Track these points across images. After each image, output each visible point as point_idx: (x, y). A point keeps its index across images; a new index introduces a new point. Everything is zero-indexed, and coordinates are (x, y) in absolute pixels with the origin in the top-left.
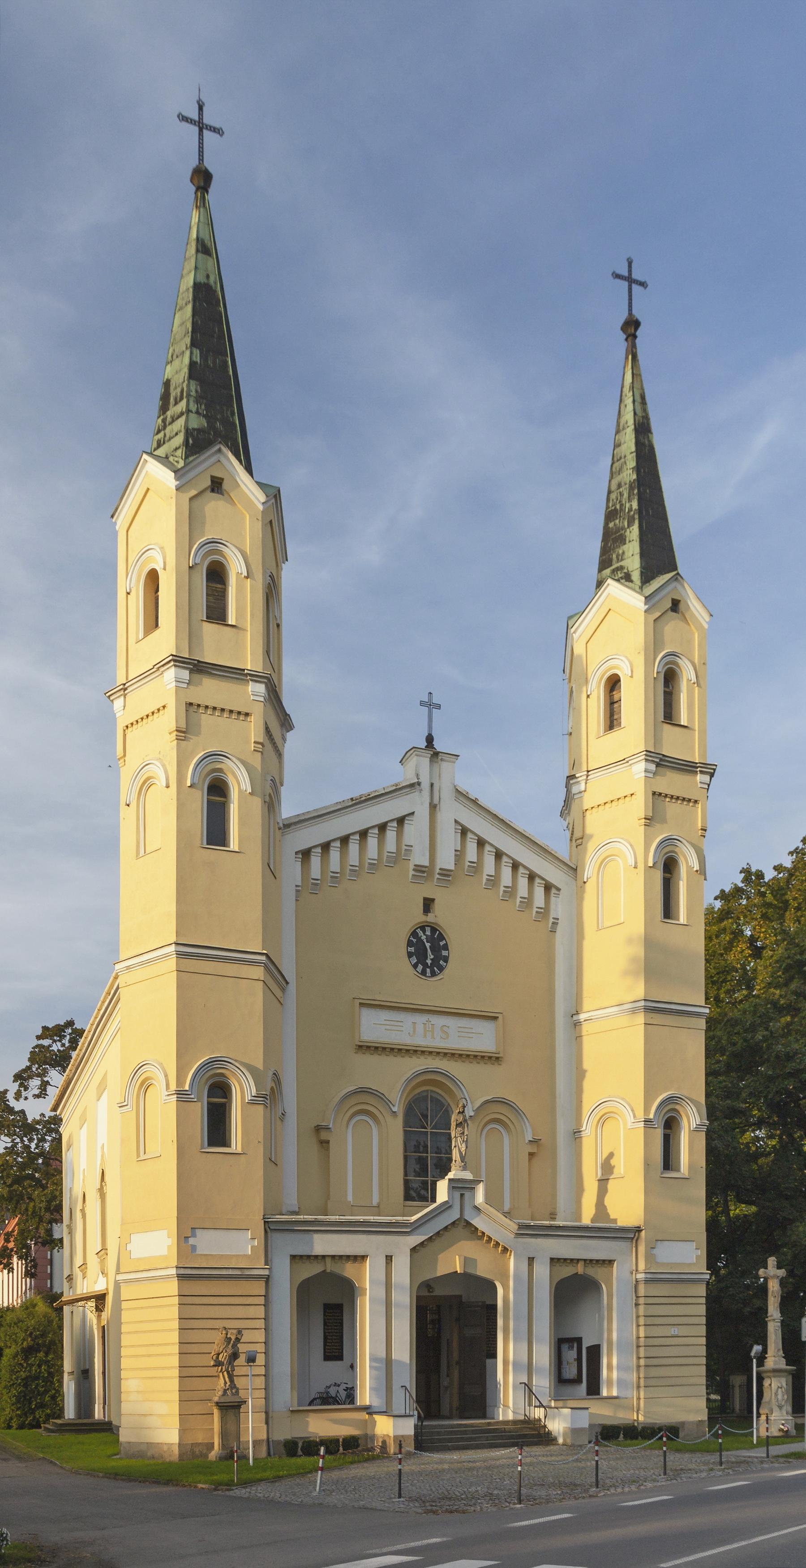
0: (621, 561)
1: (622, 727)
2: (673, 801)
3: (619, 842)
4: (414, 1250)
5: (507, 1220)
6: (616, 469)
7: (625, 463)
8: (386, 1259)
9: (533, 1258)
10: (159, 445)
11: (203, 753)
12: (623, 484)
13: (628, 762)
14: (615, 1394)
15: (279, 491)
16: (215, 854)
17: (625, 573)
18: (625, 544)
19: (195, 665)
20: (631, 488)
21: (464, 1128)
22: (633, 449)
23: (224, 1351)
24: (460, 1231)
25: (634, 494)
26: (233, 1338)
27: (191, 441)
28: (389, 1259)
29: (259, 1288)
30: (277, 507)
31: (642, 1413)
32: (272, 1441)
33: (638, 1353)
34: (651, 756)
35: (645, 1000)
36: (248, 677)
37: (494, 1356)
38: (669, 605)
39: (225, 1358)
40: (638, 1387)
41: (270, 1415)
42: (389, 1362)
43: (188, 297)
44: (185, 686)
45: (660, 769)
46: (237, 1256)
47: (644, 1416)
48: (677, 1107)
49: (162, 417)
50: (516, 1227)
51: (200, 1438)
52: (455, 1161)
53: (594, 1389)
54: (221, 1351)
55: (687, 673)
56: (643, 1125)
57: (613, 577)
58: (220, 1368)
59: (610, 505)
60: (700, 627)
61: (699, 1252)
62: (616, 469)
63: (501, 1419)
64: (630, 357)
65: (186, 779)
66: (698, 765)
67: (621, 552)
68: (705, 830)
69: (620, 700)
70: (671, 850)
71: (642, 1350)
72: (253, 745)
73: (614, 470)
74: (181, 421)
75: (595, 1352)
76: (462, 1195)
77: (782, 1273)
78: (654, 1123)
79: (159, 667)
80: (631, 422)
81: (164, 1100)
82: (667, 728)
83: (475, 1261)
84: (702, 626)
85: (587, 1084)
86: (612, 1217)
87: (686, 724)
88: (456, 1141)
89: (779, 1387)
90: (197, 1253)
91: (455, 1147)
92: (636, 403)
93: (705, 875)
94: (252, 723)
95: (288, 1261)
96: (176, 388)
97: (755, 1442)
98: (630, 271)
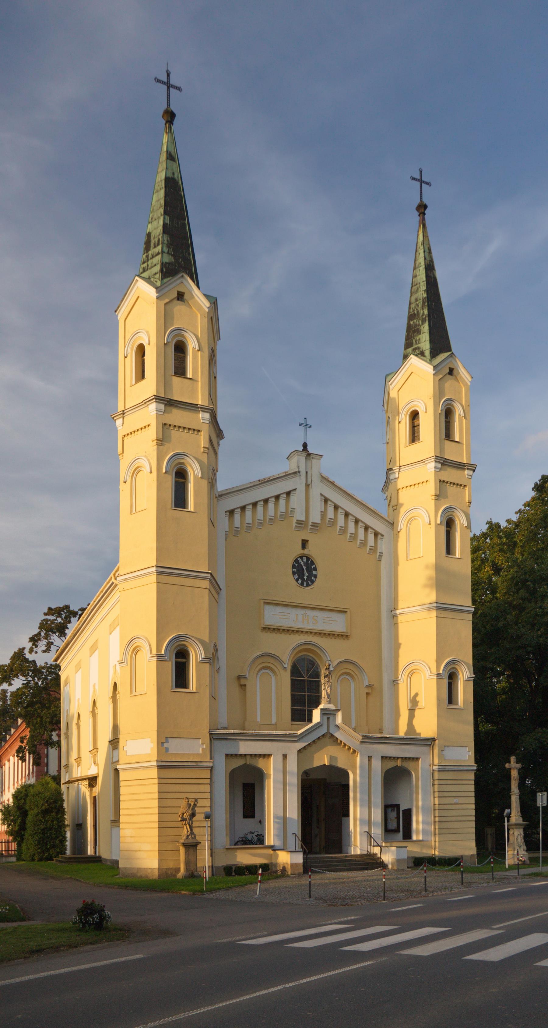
0: (418, 344)
1: (420, 441)
2: (452, 485)
3: (419, 509)
4: (299, 751)
5: (356, 734)
6: (414, 290)
7: (420, 287)
8: (283, 757)
9: (371, 756)
10: (144, 270)
11: (172, 453)
12: (418, 299)
13: (424, 462)
14: (421, 838)
15: (216, 300)
16: (179, 513)
17: (421, 351)
18: (420, 334)
19: (168, 402)
20: (423, 302)
21: (329, 678)
22: (424, 279)
23: (187, 812)
24: (327, 740)
25: (425, 306)
26: (192, 804)
27: (164, 270)
28: (285, 756)
29: (207, 774)
30: (215, 309)
31: (438, 850)
32: (215, 867)
33: (434, 814)
34: (438, 459)
35: (436, 603)
36: (200, 409)
37: (347, 815)
38: (448, 371)
39: (188, 816)
40: (435, 834)
41: (214, 850)
42: (285, 818)
43: (162, 185)
44: (162, 413)
45: (444, 467)
47: (439, 852)
48: (456, 666)
49: (146, 254)
50: (361, 738)
51: (171, 865)
52: (324, 698)
53: (407, 835)
54: (185, 812)
55: (458, 411)
56: (436, 677)
57: (414, 353)
58: (184, 822)
59: (411, 311)
60: (465, 384)
61: (470, 753)
62: (414, 290)
63: (352, 853)
64: (422, 226)
65: (163, 469)
66: (466, 465)
67: (418, 338)
68: (471, 503)
69: (419, 425)
70: (449, 514)
71: (437, 812)
72: (202, 449)
73: (413, 290)
74: (158, 258)
75: (408, 814)
76: (328, 718)
77: (519, 766)
79: (146, 402)
80: (423, 263)
81: (150, 660)
82: (447, 442)
83: (336, 758)
84: (467, 384)
85: (402, 652)
87: (458, 441)
88: (324, 686)
89: (518, 835)
90: (169, 752)
91: (324, 689)
92: (426, 253)
93: (471, 529)
94: (202, 436)
95: (224, 757)
96: (154, 238)
97: (507, 867)
98: (421, 176)
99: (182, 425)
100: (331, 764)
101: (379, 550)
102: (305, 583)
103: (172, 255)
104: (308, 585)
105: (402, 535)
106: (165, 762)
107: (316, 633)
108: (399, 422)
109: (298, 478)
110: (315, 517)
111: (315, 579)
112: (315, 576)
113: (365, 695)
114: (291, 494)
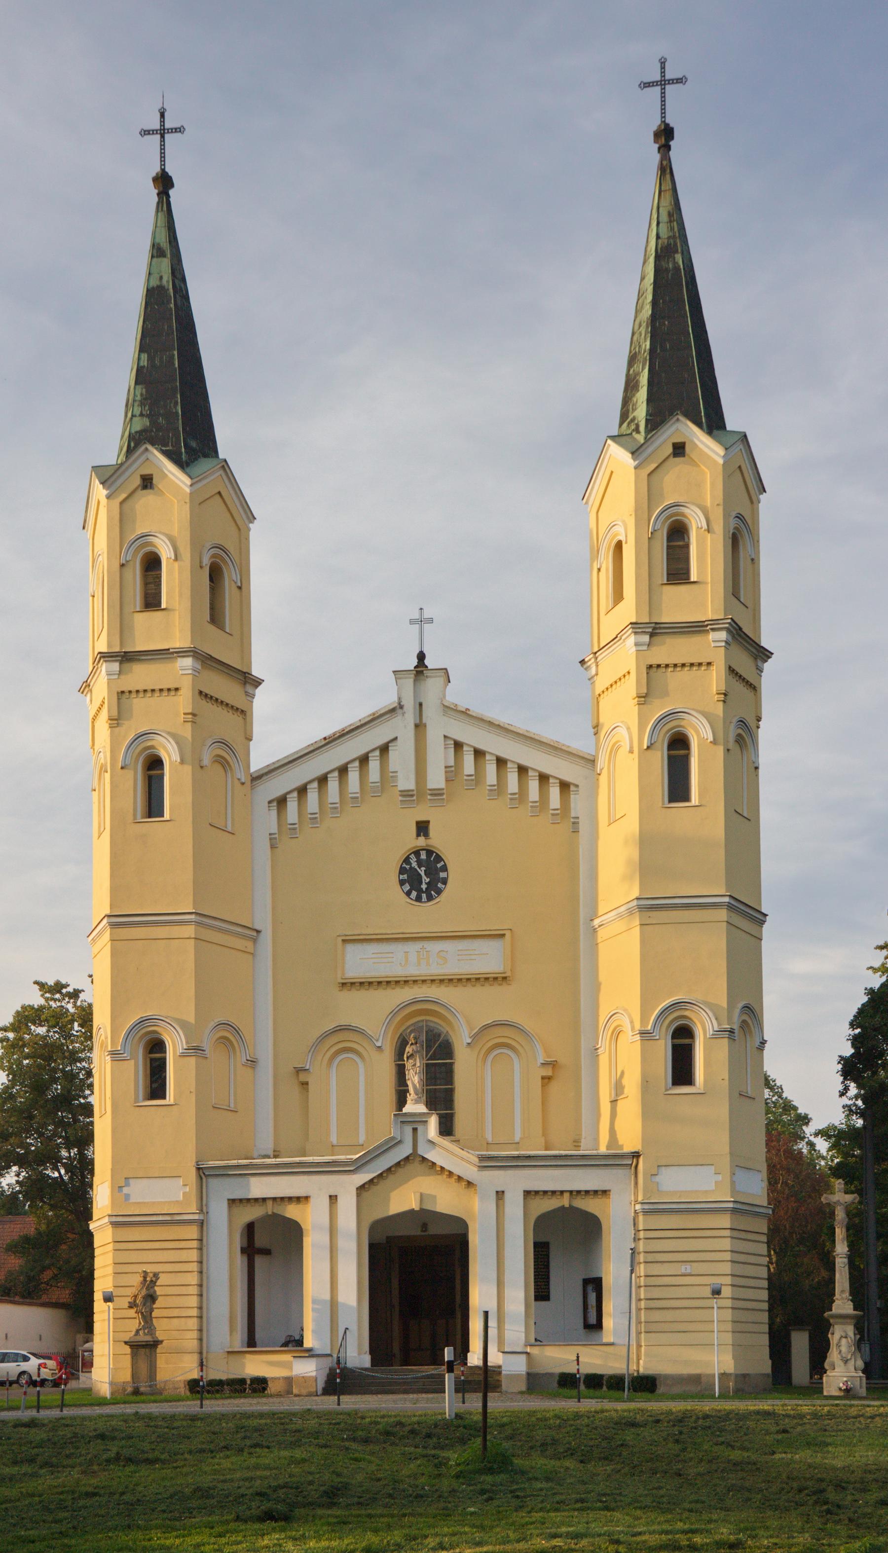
2: (678, 669)
4: (361, 1189)
7: (646, 297)
9: (503, 1192)
16: (153, 826)
18: (638, 391)
20: (647, 327)
21: (415, 1060)
22: (652, 281)
24: (416, 1166)
27: (132, 444)
28: (333, 1199)
29: (192, 1232)
42: (334, 1304)
45: (655, 639)
46: (169, 1203)
48: (687, 1013)
50: (477, 1160)
56: (639, 1038)
61: (720, 1177)
72: (183, 716)
76: (415, 1130)
78: (654, 1034)
84: (715, 462)
86: (620, 1143)
90: (132, 1201)
92: (661, 225)
95: (225, 1205)
99: (149, 688)
100: (424, 1207)
101: (573, 815)
102: (424, 896)
103: (148, 416)
104: (430, 898)
105: (603, 780)
106: (121, 1217)
107: (442, 981)
108: (599, 570)
109: (400, 717)
110: (436, 779)
111: (444, 886)
112: (445, 881)
113: (539, 1082)
114: (390, 748)
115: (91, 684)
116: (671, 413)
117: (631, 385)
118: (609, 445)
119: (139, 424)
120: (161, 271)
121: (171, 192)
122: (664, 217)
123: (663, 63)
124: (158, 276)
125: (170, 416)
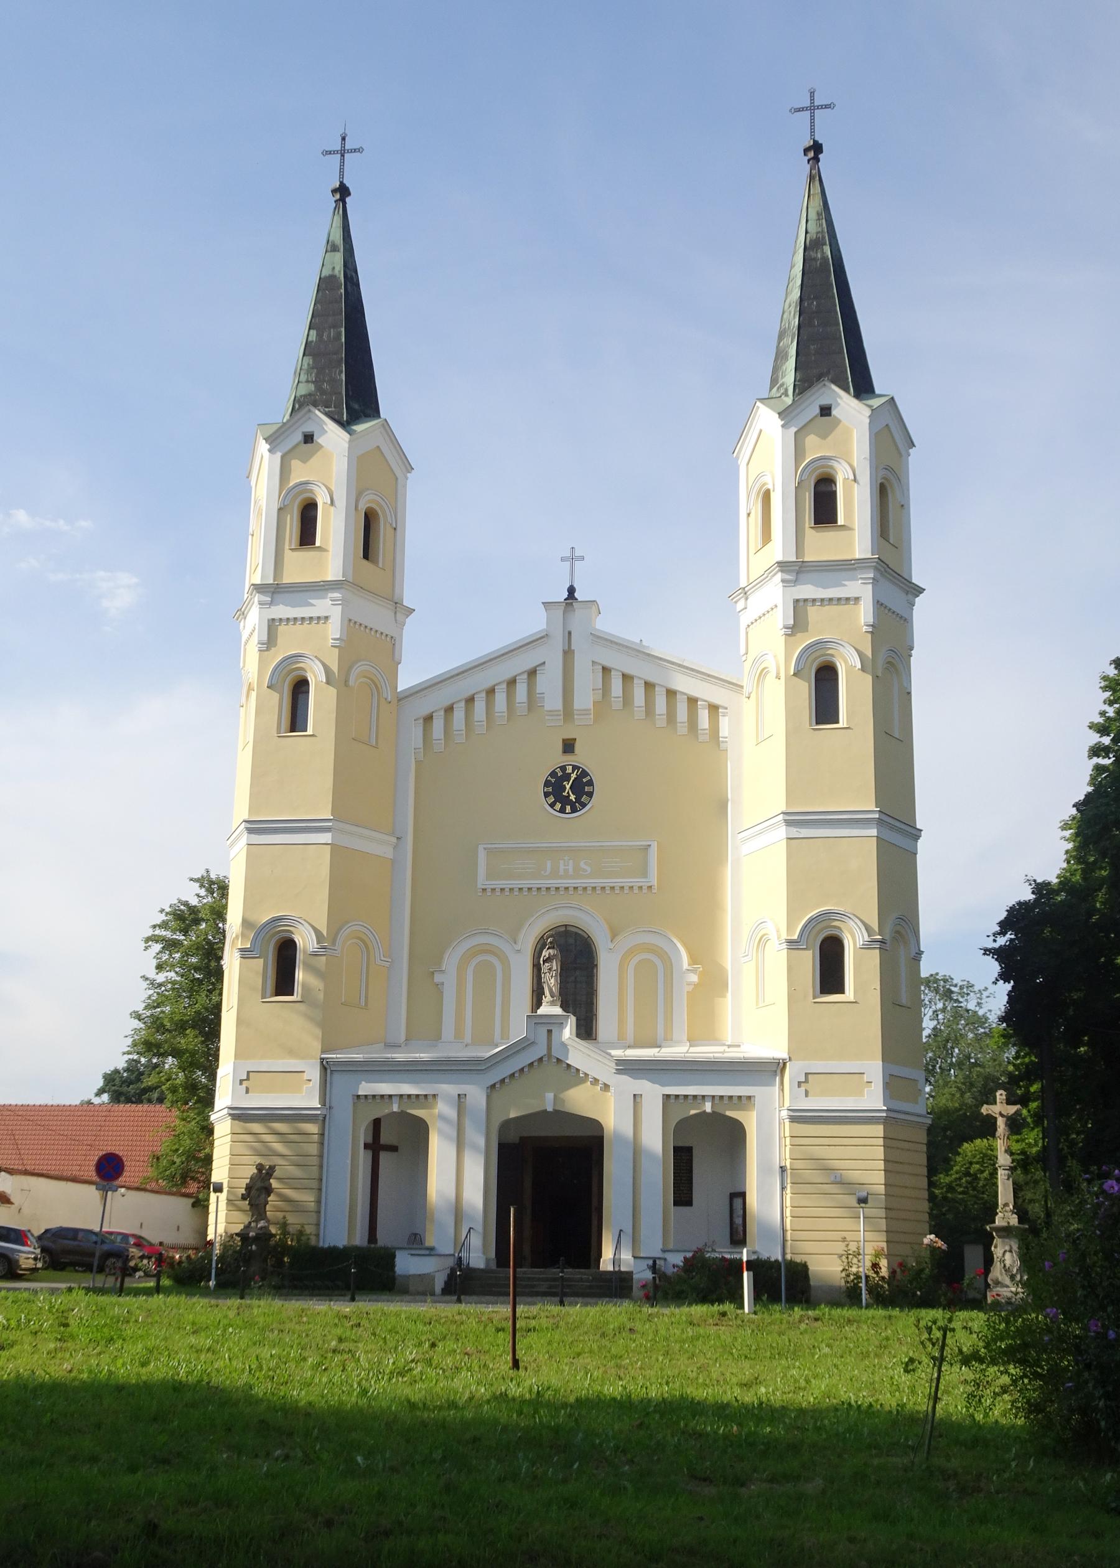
27: (297, 406)
76: (550, 1032)
100: (557, 1108)
103: (312, 382)
115: (245, 613)
116: (819, 377)
117: (780, 356)
118: (758, 407)
119: (304, 389)
120: (334, 263)
121: (348, 200)
122: (813, 215)
123: (812, 94)
124: (331, 267)
125: (334, 382)
